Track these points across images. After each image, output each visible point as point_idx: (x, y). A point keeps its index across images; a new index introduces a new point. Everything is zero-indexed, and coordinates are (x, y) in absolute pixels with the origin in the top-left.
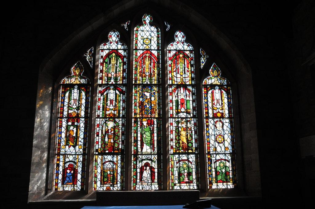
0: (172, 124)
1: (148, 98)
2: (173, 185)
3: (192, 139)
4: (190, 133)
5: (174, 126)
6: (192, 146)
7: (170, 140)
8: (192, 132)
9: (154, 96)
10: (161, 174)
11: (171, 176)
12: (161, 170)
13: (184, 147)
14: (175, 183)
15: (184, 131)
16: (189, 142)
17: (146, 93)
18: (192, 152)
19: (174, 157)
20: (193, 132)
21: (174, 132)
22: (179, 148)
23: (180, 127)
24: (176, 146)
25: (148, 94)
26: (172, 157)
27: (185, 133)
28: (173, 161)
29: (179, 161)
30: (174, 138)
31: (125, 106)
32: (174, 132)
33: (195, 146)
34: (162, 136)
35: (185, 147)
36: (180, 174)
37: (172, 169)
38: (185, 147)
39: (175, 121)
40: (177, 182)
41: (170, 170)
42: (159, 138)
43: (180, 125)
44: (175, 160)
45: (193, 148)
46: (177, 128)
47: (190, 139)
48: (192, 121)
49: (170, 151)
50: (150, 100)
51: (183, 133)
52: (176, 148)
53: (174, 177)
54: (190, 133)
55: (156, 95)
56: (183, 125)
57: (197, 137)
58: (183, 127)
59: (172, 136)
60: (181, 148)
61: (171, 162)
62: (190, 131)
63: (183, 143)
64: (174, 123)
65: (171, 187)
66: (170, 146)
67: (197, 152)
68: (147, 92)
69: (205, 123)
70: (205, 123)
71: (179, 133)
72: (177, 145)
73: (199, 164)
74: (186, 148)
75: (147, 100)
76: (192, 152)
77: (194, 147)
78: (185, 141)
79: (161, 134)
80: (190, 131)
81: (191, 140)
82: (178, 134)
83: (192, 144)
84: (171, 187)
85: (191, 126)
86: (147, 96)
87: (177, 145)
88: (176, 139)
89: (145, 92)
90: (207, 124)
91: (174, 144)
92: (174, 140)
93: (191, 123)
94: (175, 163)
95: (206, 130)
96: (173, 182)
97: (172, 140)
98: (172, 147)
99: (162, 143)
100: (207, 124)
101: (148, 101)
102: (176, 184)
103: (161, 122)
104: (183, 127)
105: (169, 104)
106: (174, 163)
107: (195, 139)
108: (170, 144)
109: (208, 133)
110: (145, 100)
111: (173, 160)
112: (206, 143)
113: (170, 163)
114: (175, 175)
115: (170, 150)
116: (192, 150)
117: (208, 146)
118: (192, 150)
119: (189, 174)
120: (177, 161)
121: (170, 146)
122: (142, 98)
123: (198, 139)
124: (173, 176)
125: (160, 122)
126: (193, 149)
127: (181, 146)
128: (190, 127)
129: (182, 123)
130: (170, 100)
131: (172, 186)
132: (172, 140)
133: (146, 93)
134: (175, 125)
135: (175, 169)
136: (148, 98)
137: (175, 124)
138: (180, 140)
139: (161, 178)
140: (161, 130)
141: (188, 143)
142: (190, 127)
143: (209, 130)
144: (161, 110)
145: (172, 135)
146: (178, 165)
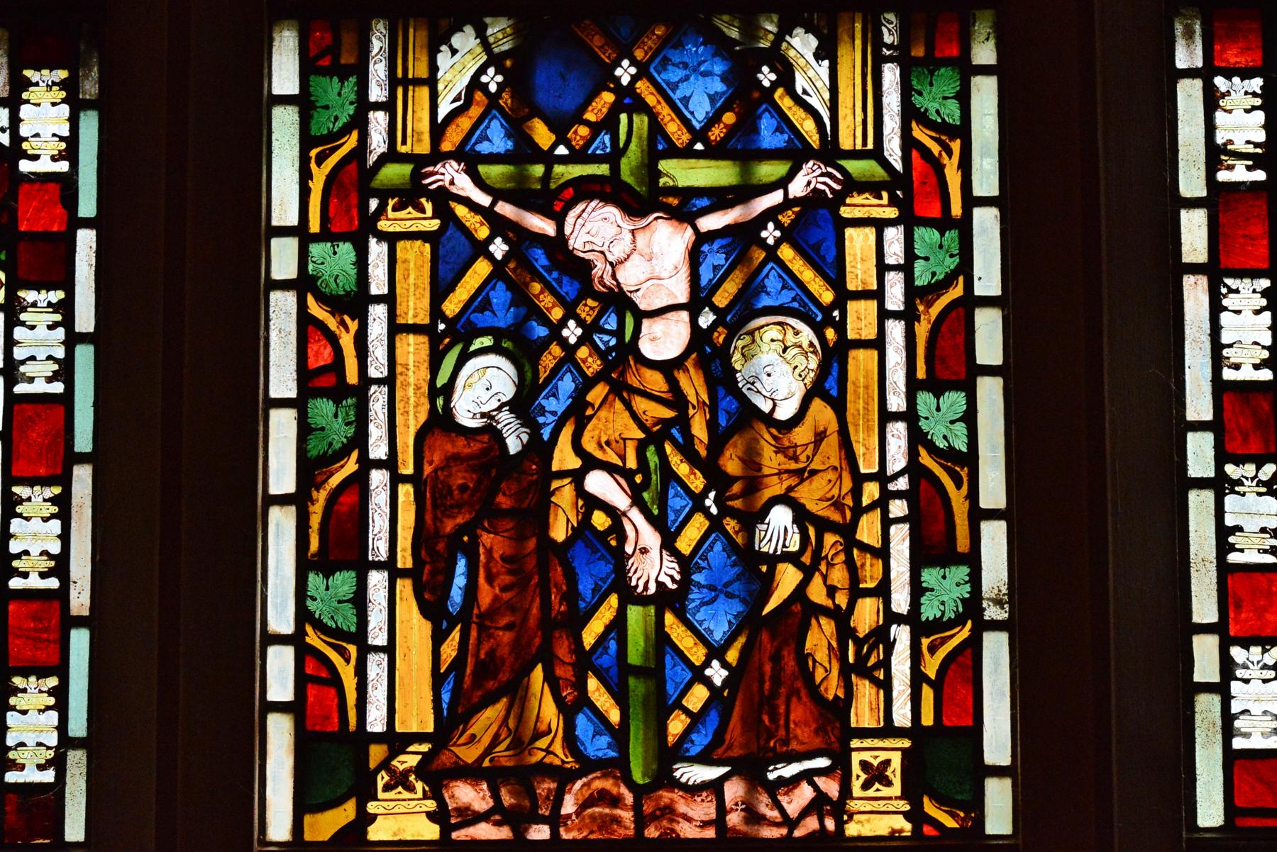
1: (665, 339)
9: (805, 307)
17: (596, 229)
25: (651, 260)
31: (81, 568)
50: (693, 385)
55: (860, 272)
68: (642, 200)
75: (622, 391)
86: (619, 301)
89: (585, 190)
101: (654, 436)
105: (1200, 504)
110: (578, 413)
122: (521, 351)
130: (1220, 388)
133: (596, 229)
136: (665, 339)
144: (996, 648)
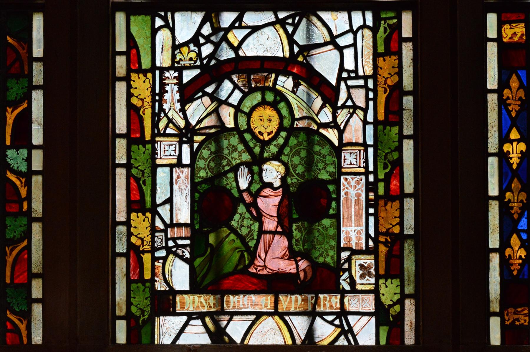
2: (141, 301)
10: (29, 198)
11: (121, 217)
12: (29, 160)
14: (160, 286)
19: (163, 37)
26: (143, 43)
28: (153, 68)
29: (214, 72)
36: (214, 203)
37: (141, 153)
40: (179, 275)
41: (121, 158)
44: (163, 59)
53: (154, 230)
61: (127, 79)
65: (121, 327)
73: (408, 102)
84: (121, 327)
94: (172, 95)
96: (141, 279)
102: (173, 292)
106: (158, 96)
111: (146, 64)
113: (121, 88)
114: (164, 211)
119: (310, 203)
120: (188, 76)
124: (141, 224)
131: (129, 317)
135: (168, 150)
139: (28, 234)
146: (197, 110)
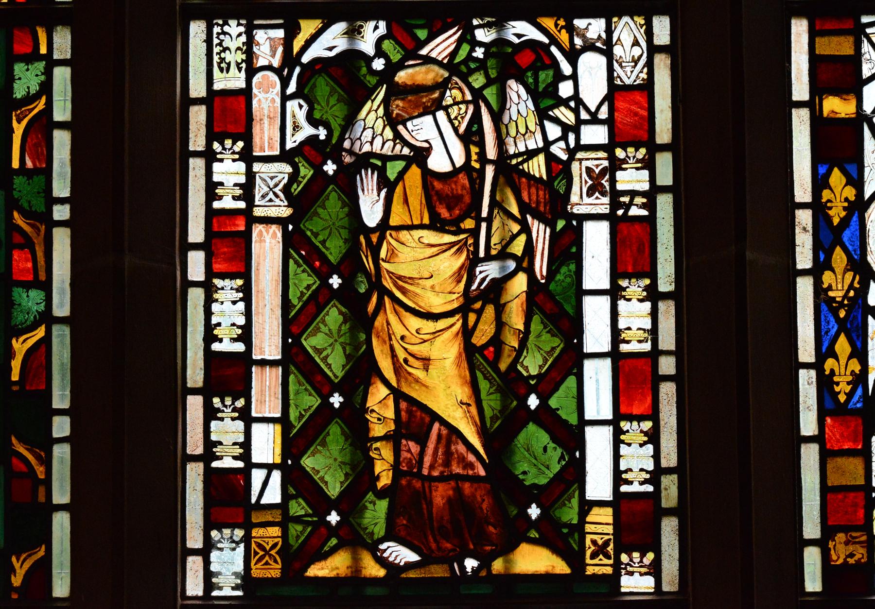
0: (232, 116)
3: (571, 360)
4: (541, 266)
5: (266, 138)
6: (575, 472)
7: (195, 376)
8: (568, 248)
13: (424, 497)
15: (436, 224)
16: (526, 416)
18: (561, 567)
20: (596, 239)
21: (267, 247)
22: (351, 501)
23: (364, 161)
24: (296, 479)
27: (450, 264)
30: (268, 343)
32: (267, 247)
33: (619, 477)
34: (62, 307)
35: (440, 495)
38: (440, 495)
39: (290, 60)
42: (20, 346)
43: (371, 131)
45: (586, 506)
46: (324, 175)
47: (532, 364)
48: (573, 56)
49: (194, 564)
51: (425, 264)
52: (298, 508)
54: (541, 266)
56: (422, 130)
57: (654, 332)
58: (420, 155)
59: (244, 311)
60: (376, 514)
62: (540, 233)
63: (415, 420)
64: (266, 96)
66: (194, 473)
67: (655, 570)
69: (800, 90)
70: (800, 90)
71: (350, 265)
72: (326, 466)
74: (457, 502)
76: (561, 567)
77: (598, 485)
78: (446, 392)
79: (46, 286)
80: (540, 233)
81: (547, 384)
82: (344, 282)
83: (571, 438)
85: (558, 150)
87: (326, 466)
88: (294, 359)
90: (836, 106)
91: (266, 444)
92: (266, 391)
93: (565, 89)
95: (818, 207)
97: (230, 376)
98: (229, 498)
99: (61, 427)
100: (836, 106)
103: (62, 76)
104: (420, 155)
107: (615, 355)
108: (195, 445)
109: (839, 258)
112: (808, 425)
115: (195, 540)
116: (563, 539)
117: (849, 471)
118: (563, 539)
121: (194, 473)
123: (667, 365)
125: (46, 88)
126: (579, 528)
127: (385, 480)
128: (537, 167)
129: (425, 98)
132: (230, 376)
134: (279, 118)
137: (297, 110)
138: (362, 370)
140: (61, 212)
141: (500, 436)
142: (537, 167)
143: (859, 207)
145: (227, 289)
